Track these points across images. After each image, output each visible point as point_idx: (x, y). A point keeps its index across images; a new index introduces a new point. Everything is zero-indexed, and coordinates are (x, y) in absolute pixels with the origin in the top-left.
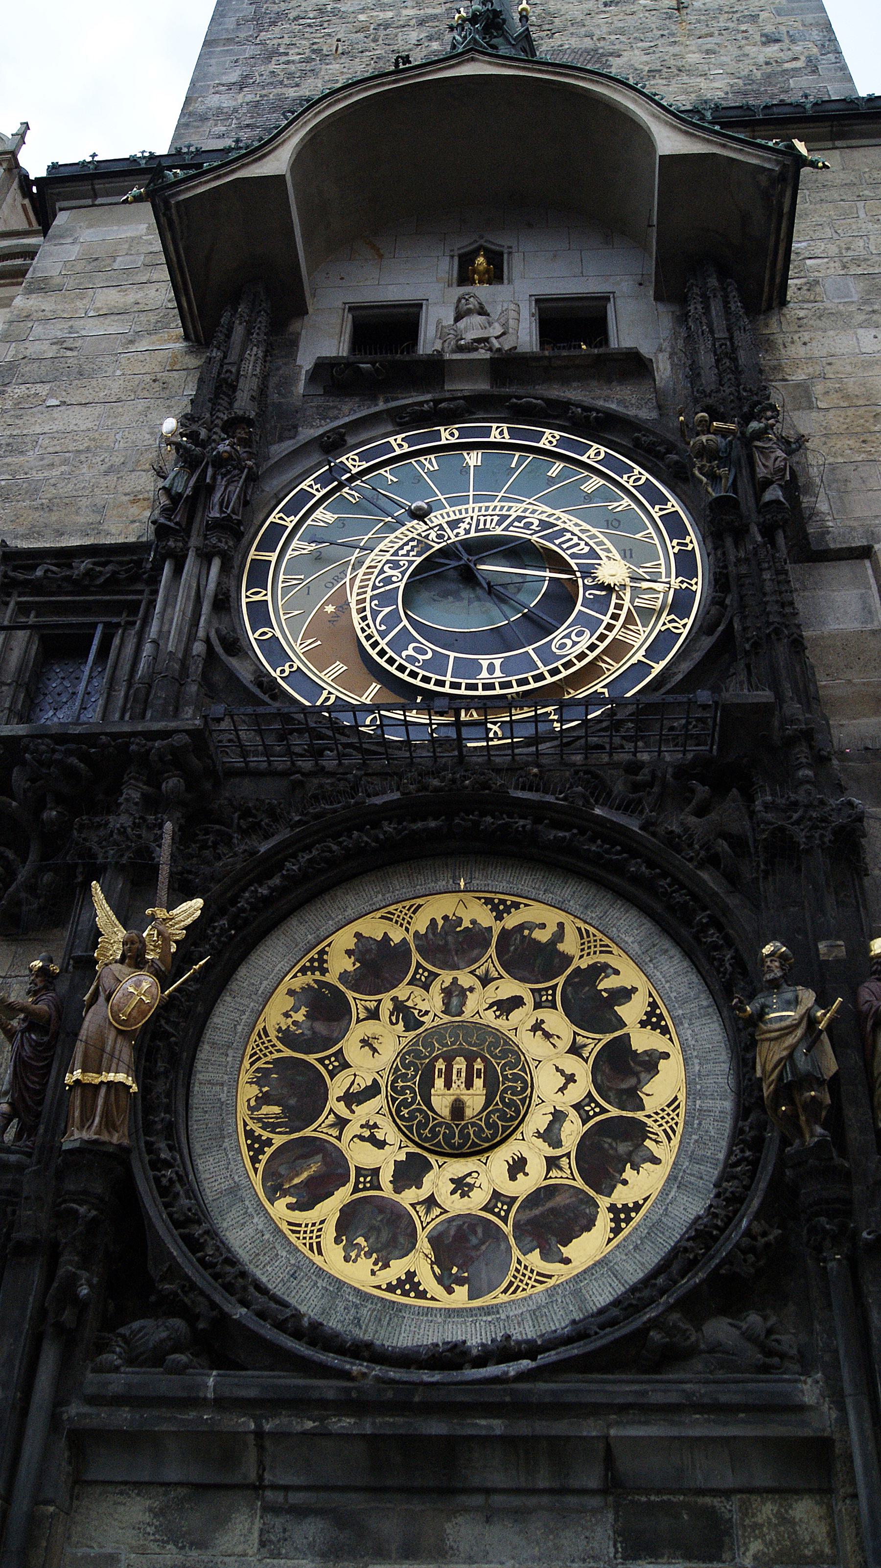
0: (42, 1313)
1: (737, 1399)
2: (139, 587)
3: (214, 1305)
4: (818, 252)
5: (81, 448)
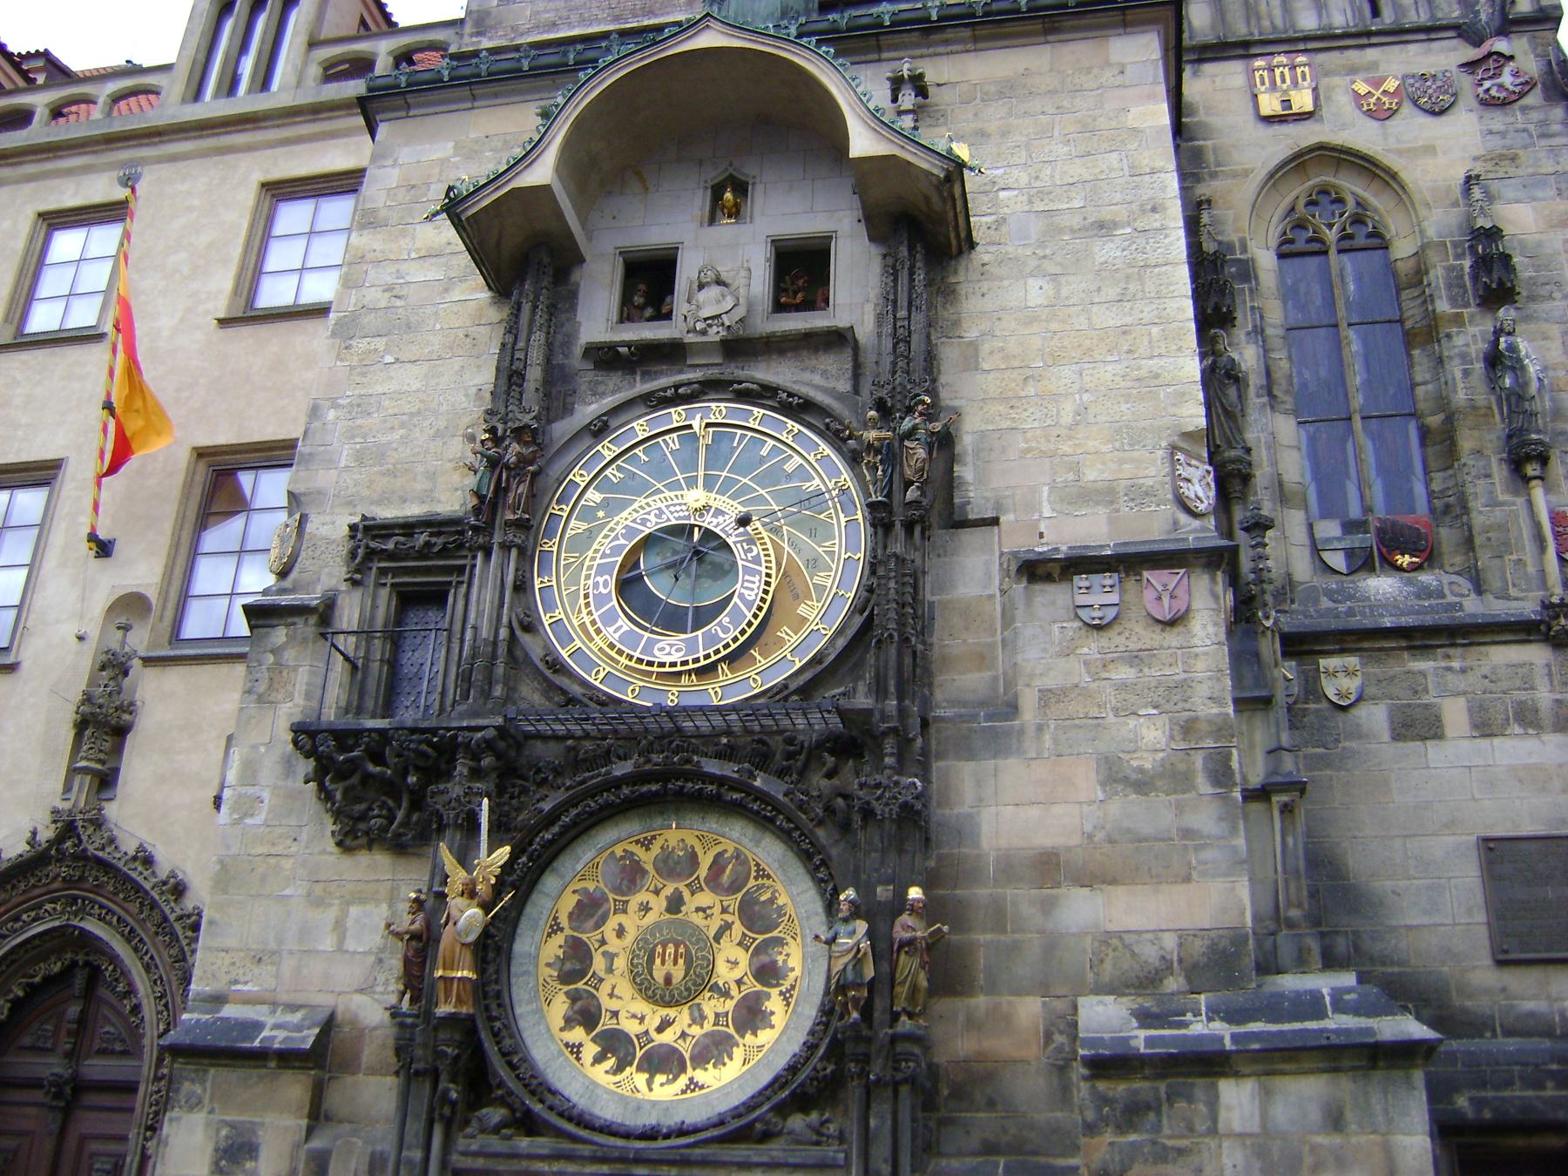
0: (431, 1110)
1: (798, 1161)
2: (464, 553)
3: (523, 1104)
4: (1011, 182)
5: (414, 410)
